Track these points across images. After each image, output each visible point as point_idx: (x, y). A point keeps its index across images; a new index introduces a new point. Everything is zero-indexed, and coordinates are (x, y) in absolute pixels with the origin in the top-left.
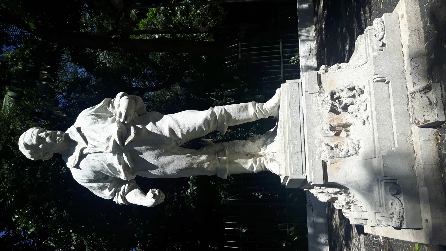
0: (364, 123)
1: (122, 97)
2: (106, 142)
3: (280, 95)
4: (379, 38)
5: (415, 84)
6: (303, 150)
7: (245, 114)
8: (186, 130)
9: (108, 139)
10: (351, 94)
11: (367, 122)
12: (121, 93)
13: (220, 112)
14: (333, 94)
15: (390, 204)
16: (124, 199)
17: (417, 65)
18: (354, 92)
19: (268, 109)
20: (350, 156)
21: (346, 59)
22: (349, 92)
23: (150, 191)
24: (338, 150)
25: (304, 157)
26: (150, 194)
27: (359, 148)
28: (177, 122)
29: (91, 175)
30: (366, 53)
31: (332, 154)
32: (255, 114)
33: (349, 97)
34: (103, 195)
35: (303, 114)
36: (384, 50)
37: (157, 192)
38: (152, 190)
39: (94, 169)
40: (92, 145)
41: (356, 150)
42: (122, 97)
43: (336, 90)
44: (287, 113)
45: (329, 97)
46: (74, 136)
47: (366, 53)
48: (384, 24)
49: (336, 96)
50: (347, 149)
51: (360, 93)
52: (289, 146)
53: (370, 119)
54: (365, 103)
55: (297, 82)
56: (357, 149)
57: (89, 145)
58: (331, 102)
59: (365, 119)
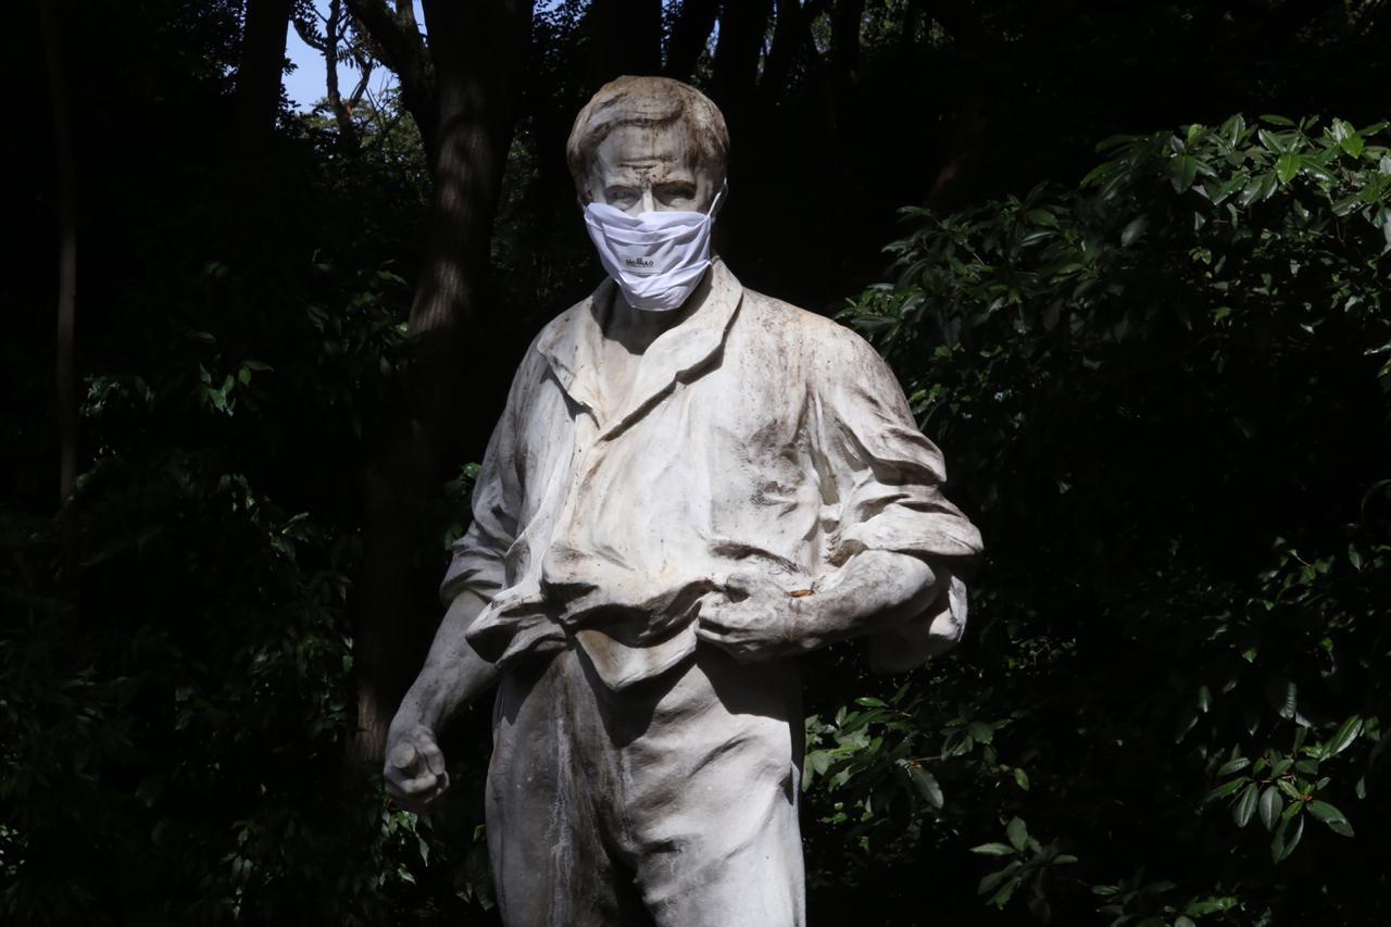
2: (596, 541)
9: (607, 552)
12: (958, 535)
34: (488, 471)
37: (426, 780)
38: (434, 755)
40: (593, 472)
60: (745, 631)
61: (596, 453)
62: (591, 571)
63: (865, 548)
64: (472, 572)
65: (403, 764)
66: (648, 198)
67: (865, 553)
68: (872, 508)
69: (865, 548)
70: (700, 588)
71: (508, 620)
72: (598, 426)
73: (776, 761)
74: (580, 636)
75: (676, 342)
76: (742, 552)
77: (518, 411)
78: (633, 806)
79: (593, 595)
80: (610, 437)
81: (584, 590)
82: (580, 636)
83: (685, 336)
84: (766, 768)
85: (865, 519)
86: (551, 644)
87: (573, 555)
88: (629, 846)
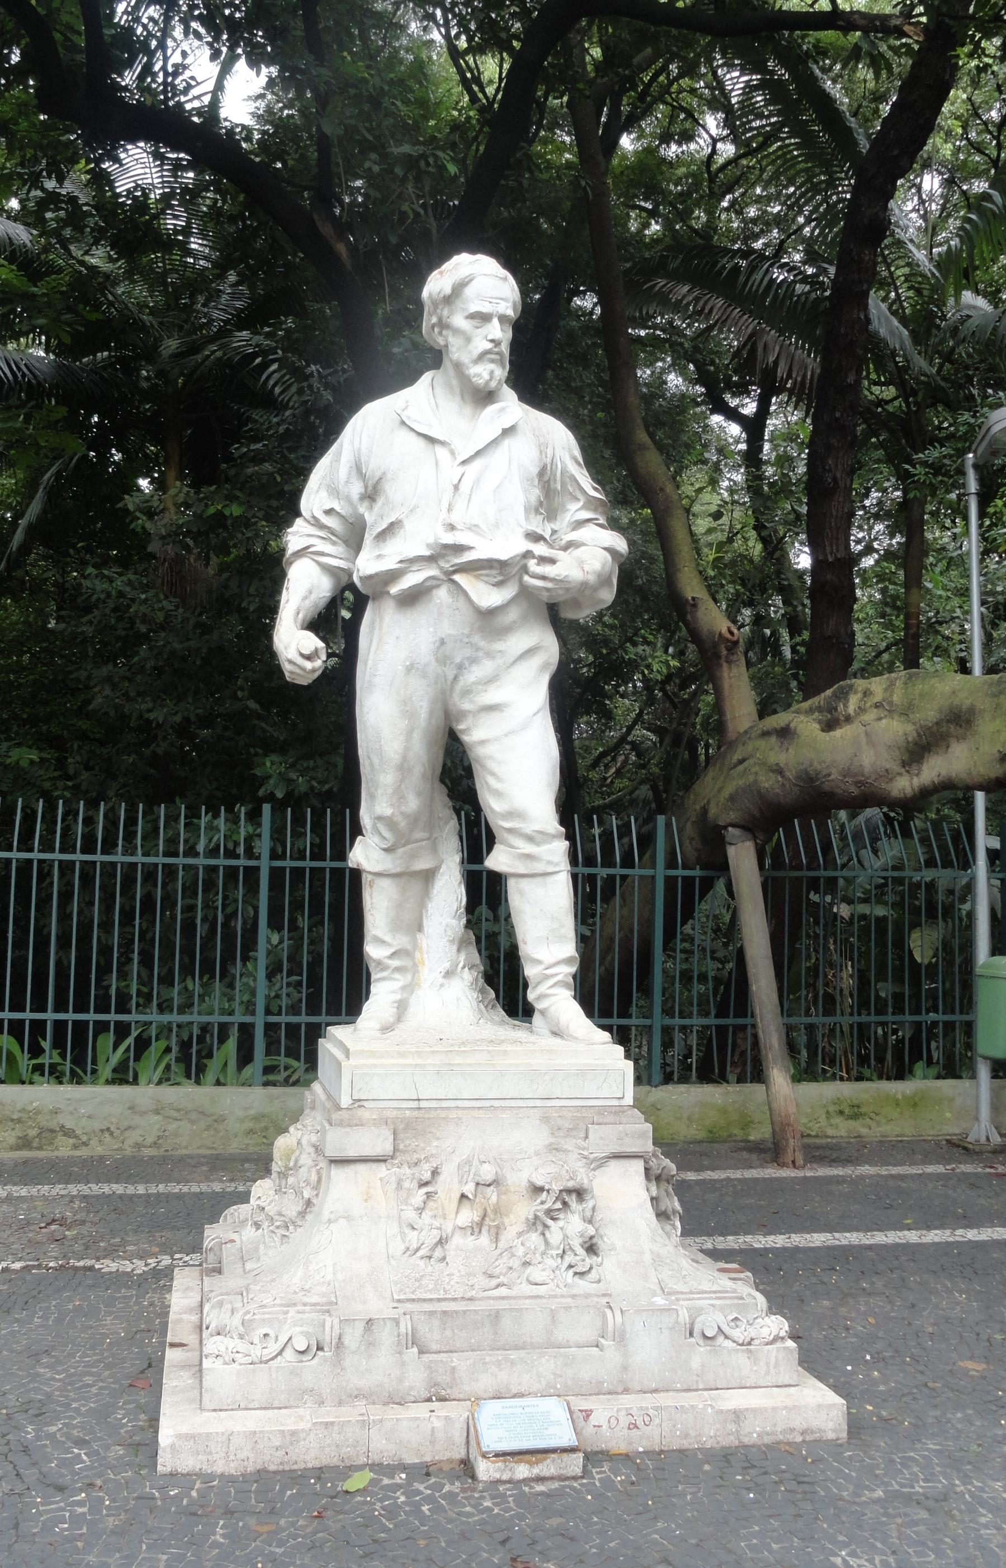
9: (474, 528)
10: (576, 1244)
13: (550, 858)
14: (580, 1193)
16: (300, 553)
17: (640, 1423)
18: (581, 1251)
20: (402, 1234)
22: (580, 1240)
23: (321, 644)
26: (312, 642)
28: (524, 727)
29: (373, 467)
32: (539, 962)
33: (566, 1237)
36: (692, 1340)
39: (389, 476)
41: (418, 1250)
45: (570, 1184)
47: (691, 1292)
49: (572, 1200)
51: (579, 1269)
53: (503, 1291)
56: (420, 1253)
57: (461, 469)
58: (556, 1187)
60: (561, 581)
62: (460, 538)
63: (584, 544)
64: (308, 547)
65: (306, 652)
67: (583, 548)
68: (580, 524)
69: (584, 544)
70: (528, 554)
72: (452, 453)
74: (457, 577)
76: (536, 537)
77: (364, 450)
78: (474, 683)
80: (464, 463)
82: (457, 577)
83: (503, 409)
85: (573, 530)
86: (434, 582)
87: (452, 528)
88: (466, 706)
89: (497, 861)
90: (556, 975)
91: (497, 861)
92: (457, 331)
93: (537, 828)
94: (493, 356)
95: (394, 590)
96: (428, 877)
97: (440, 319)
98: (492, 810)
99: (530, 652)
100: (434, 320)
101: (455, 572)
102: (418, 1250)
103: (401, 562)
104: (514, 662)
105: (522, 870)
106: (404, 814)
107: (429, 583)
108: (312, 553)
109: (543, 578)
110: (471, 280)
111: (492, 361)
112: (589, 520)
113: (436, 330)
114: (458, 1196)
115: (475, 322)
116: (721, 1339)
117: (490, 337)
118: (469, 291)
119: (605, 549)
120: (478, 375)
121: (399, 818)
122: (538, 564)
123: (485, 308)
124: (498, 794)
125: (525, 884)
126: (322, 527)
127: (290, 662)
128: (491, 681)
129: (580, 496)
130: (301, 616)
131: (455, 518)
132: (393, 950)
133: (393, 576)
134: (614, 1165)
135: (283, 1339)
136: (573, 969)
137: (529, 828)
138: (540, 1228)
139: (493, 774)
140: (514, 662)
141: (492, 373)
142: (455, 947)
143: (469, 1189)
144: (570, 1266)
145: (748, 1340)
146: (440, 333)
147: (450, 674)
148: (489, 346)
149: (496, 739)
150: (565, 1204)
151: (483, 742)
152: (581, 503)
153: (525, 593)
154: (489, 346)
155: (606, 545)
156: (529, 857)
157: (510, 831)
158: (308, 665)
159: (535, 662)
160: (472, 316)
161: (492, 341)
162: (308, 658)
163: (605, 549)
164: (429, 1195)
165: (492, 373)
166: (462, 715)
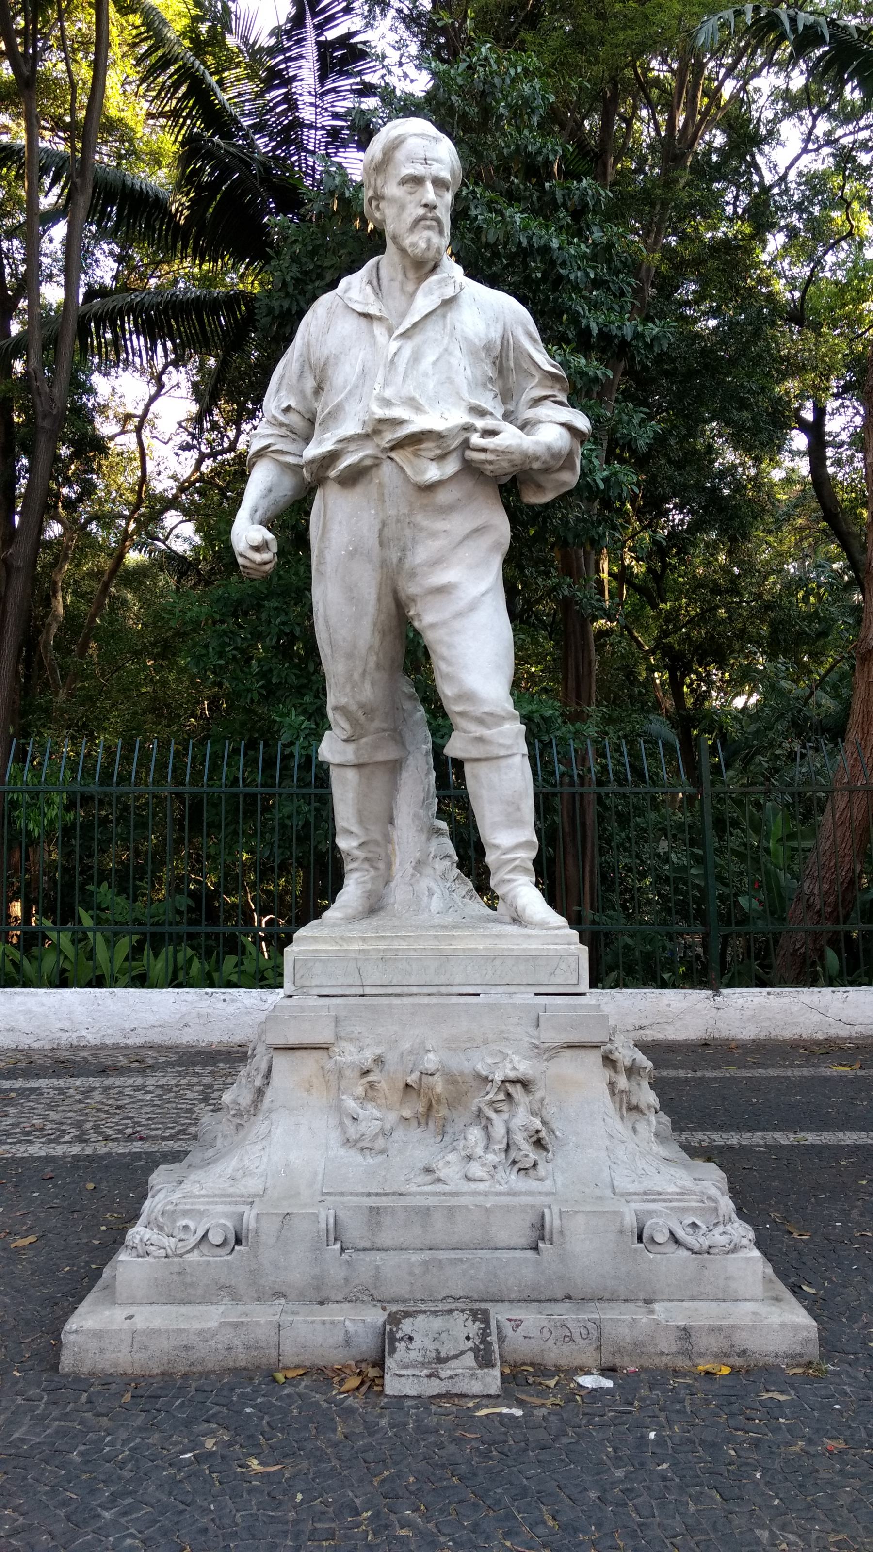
0: (428, 1170)
1: (569, 427)
3: (543, 925)
4: (680, 1233)
5: (518, 1326)
6: (368, 990)
7: (497, 819)
8: (446, 638)
11: (429, 1178)
12: (582, 422)
13: (501, 741)
14: (524, 1084)
15: (184, 1222)
16: (261, 454)
17: (576, 1336)
19: (511, 890)
20: (341, 1123)
21: (700, 1138)
22: (525, 1134)
23: (270, 536)
24: (360, 1091)
25: (347, 993)
26: (260, 534)
27: (362, 1149)
28: (472, 607)
29: (320, 353)
30: (645, 1193)
31: (348, 1073)
32: (497, 847)
35: (478, 995)
36: (642, 1245)
39: (332, 361)
42: (569, 427)
43: (539, 1095)
44: (481, 947)
45: (512, 1075)
46: (431, 292)
48: (728, 1253)
49: (517, 1091)
50: (361, 1118)
52: (379, 950)
53: (439, 1187)
54: (486, 1177)
55: (581, 981)
56: (361, 1144)
58: (498, 1077)
59: (441, 1174)
61: (394, 346)
62: (398, 412)
64: (268, 446)
65: (255, 544)
66: (429, 185)
68: (537, 402)
70: (468, 428)
71: (340, 446)
73: (502, 540)
74: (393, 455)
75: (440, 282)
78: (419, 565)
79: (405, 426)
81: (397, 423)
84: (496, 546)
89: (454, 748)
90: (515, 859)
91: (454, 748)
92: (393, 200)
93: (486, 709)
94: (428, 223)
95: (333, 474)
96: (395, 767)
97: (375, 192)
98: (445, 696)
99: (477, 531)
100: (370, 193)
101: (392, 449)
102: (356, 1142)
103: (340, 441)
104: (461, 542)
105: (474, 754)
106: (362, 706)
107: (368, 462)
108: (272, 452)
109: (484, 450)
110: (402, 142)
111: (429, 228)
112: (545, 398)
113: (374, 203)
114: (401, 1085)
115: (407, 187)
116: (672, 1247)
117: (423, 202)
118: (400, 155)
119: (563, 425)
120: (414, 245)
121: (353, 707)
122: (482, 437)
123: (419, 170)
124: (449, 678)
125: (482, 769)
126: (282, 425)
127: (242, 555)
128: (436, 562)
129: (534, 372)
130: (259, 513)
131: (388, 393)
132: (361, 841)
133: (332, 457)
134: (568, 1053)
135: (200, 1233)
136: (533, 854)
137: (479, 710)
138: (484, 1122)
139: (443, 658)
140: (461, 542)
141: (429, 240)
142: (424, 837)
143: (412, 1079)
144: (514, 1162)
145: (705, 1247)
146: (378, 207)
147: (394, 556)
148: (421, 211)
149: (444, 623)
150: (509, 1095)
151: (432, 626)
152: (537, 380)
153: (470, 469)
154: (421, 211)
155: (563, 420)
156: (480, 740)
157: (461, 714)
158: (258, 557)
159: (485, 542)
160: (404, 181)
161: (426, 205)
162: (257, 549)
163: (563, 425)
164: (371, 1085)
165: (429, 240)
166: (413, 599)
